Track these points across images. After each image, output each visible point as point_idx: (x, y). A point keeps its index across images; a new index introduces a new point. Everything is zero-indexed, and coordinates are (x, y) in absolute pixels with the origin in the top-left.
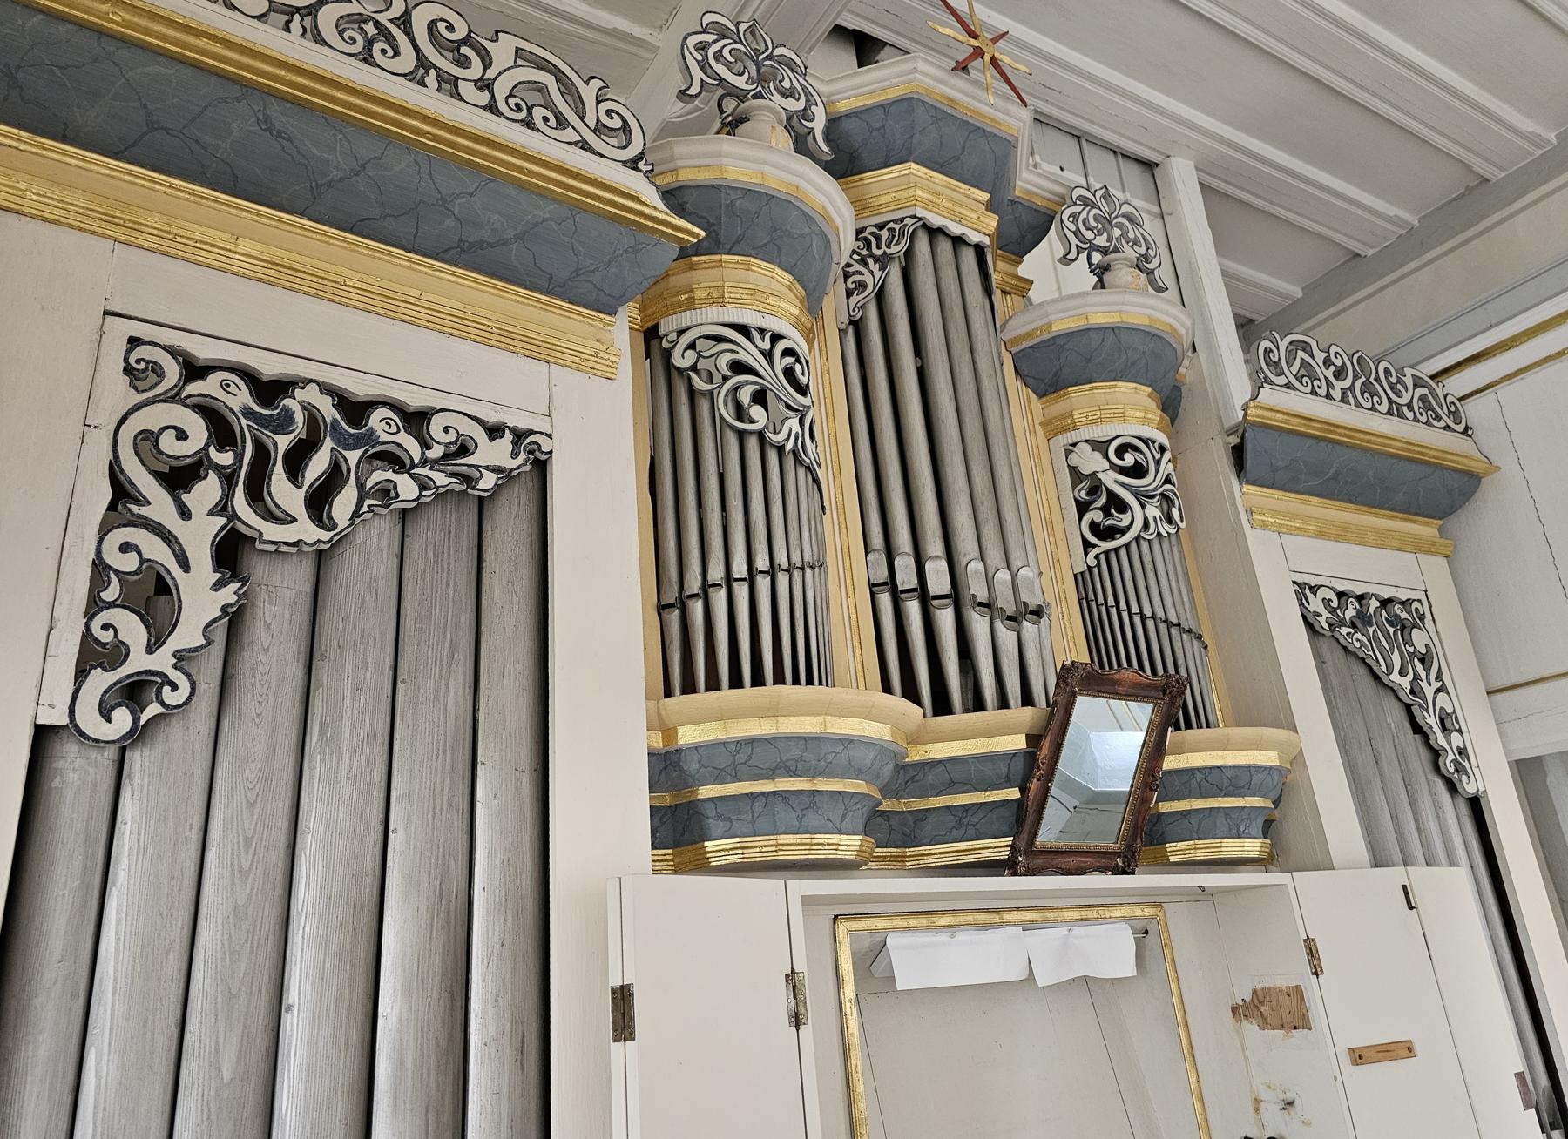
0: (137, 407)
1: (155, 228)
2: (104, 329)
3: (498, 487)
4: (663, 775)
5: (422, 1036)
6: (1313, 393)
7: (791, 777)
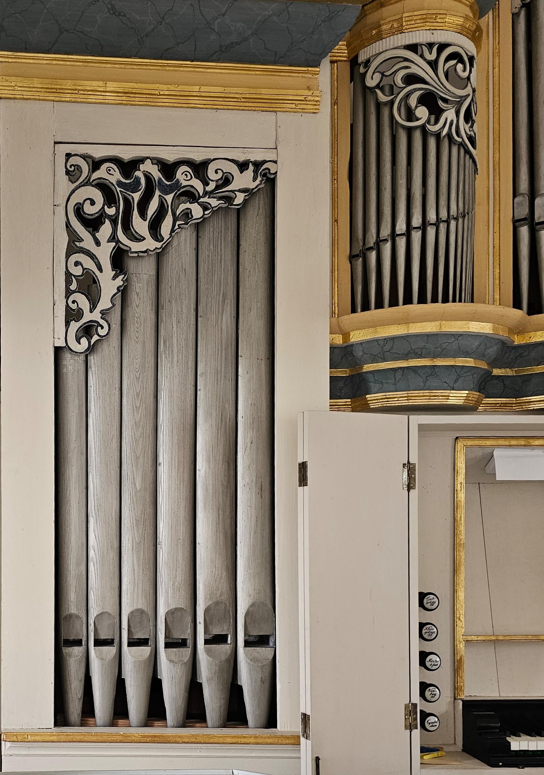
0: (73, 192)
1: (70, 89)
2: (55, 152)
3: (245, 201)
4: (344, 359)
5: (216, 480)
7: (419, 358)
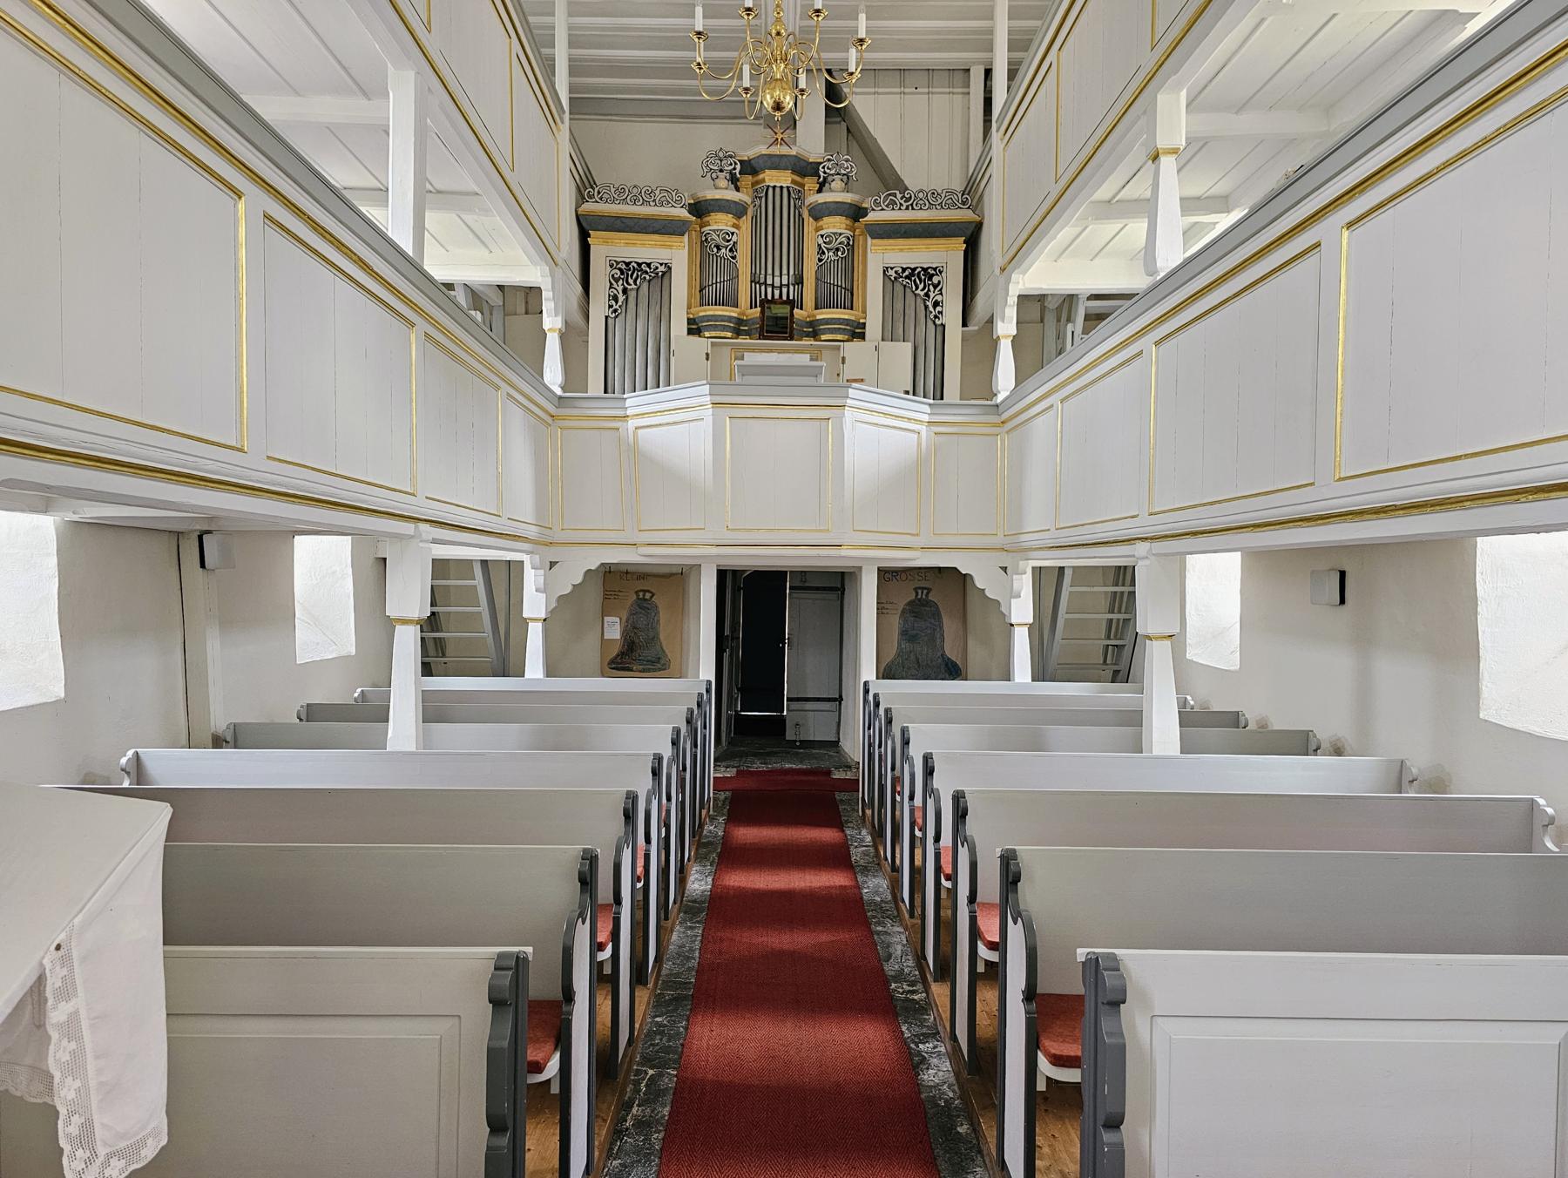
6: (893, 209)
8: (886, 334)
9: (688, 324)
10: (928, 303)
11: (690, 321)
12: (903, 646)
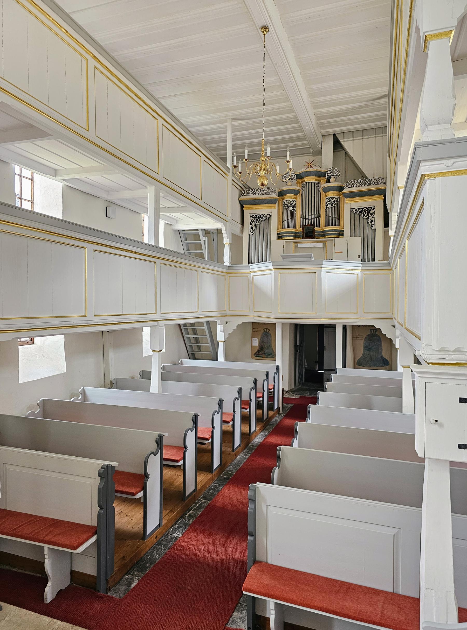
6: (353, 187)
8: (352, 234)
9: (278, 235)
10: (368, 221)
11: (278, 234)
12: (365, 352)
